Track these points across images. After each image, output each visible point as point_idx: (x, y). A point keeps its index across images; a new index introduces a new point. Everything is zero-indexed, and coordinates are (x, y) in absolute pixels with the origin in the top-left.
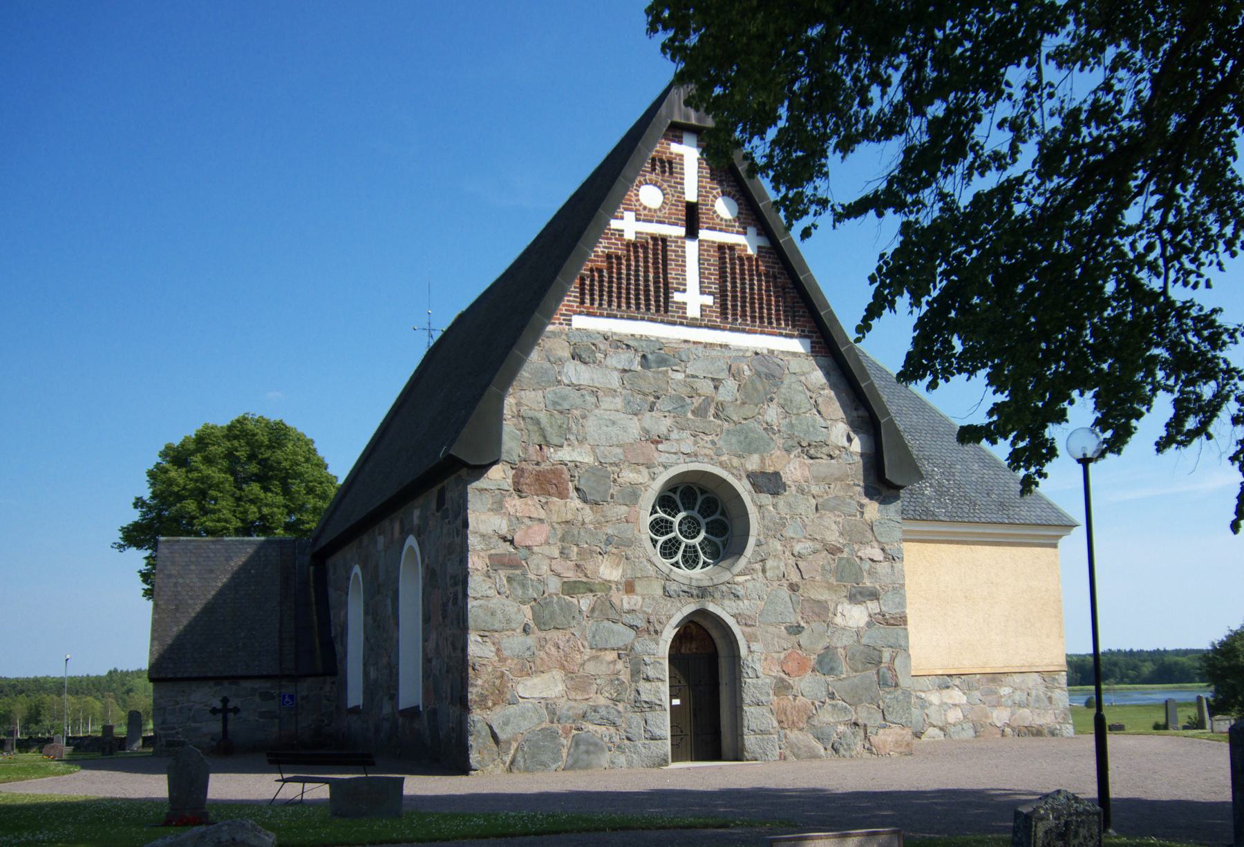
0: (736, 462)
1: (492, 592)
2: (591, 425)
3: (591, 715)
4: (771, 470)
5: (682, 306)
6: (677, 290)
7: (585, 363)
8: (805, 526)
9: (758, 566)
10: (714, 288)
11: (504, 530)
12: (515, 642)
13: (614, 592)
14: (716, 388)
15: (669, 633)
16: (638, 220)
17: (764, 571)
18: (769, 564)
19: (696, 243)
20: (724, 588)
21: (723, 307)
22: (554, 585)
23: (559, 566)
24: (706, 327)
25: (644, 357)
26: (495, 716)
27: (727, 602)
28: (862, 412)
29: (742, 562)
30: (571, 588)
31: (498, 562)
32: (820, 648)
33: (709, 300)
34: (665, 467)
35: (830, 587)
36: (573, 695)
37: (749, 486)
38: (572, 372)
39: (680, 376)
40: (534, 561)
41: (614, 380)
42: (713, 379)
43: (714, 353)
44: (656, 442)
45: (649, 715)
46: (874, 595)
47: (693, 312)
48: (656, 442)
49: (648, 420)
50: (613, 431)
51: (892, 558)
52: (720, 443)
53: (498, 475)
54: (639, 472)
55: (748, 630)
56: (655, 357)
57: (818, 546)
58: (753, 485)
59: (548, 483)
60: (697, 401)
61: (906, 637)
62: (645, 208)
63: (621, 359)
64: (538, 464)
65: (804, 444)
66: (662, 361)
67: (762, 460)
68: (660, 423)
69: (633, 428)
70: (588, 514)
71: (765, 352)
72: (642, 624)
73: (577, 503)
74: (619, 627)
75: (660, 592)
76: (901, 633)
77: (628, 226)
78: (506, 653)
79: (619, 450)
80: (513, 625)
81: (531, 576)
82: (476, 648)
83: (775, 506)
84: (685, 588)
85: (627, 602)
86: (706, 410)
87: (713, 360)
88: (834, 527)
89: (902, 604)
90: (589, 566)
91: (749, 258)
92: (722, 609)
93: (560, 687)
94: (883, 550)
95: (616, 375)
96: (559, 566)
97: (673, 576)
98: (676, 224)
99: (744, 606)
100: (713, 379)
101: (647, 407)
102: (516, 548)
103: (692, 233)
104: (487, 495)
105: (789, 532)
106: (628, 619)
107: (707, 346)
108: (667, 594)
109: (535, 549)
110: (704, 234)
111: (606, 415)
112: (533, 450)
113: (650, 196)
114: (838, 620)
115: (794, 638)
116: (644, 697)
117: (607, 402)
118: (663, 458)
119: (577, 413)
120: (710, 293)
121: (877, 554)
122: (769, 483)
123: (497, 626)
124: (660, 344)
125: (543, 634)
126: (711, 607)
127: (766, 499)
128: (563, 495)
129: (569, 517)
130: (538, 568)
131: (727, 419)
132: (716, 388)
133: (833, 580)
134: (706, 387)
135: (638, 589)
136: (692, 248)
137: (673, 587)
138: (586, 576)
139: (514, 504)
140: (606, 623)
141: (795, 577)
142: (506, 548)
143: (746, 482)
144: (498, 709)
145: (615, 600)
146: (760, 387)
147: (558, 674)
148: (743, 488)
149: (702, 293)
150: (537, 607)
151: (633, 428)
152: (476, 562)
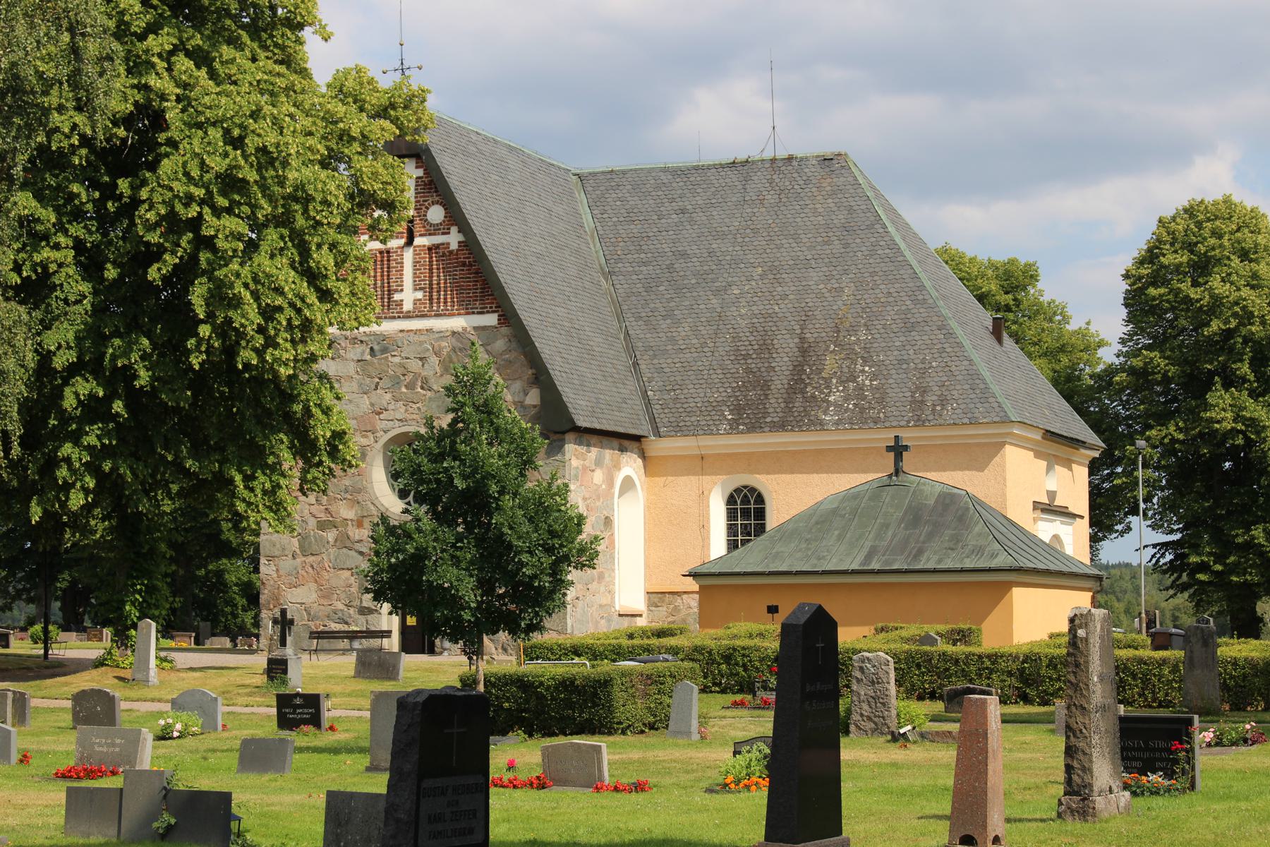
5: (400, 303)
6: (396, 291)
12: (287, 564)
19: (411, 249)
21: (431, 299)
22: (312, 523)
25: (372, 349)
30: (322, 526)
33: (420, 295)
36: (322, 601)
39: (397, 360)
41: (351, 368)
43: (422, 338)
45: (369, 617)
47: (408, 306)
49: (374, 396)
54: (366, 437)
60: (409, 378)
66: (385, 350)
69: (365, 402)
74: (352, 553)
78: (281, 573)
87: (421, 343)
91: (451, 252)
93: (314, 596)
96: (314, 509)
100: (421, 359)
103: (410, 242)
106: (357, 546)
110: (418, 241)
118: (384, 425)
123: (277, 553)
131: (430, 389)
134: (415, 365)
136: (408, 255)
140: (345, 550)
145: (350, 533)
147: (313, 586)
151: (365, 402)
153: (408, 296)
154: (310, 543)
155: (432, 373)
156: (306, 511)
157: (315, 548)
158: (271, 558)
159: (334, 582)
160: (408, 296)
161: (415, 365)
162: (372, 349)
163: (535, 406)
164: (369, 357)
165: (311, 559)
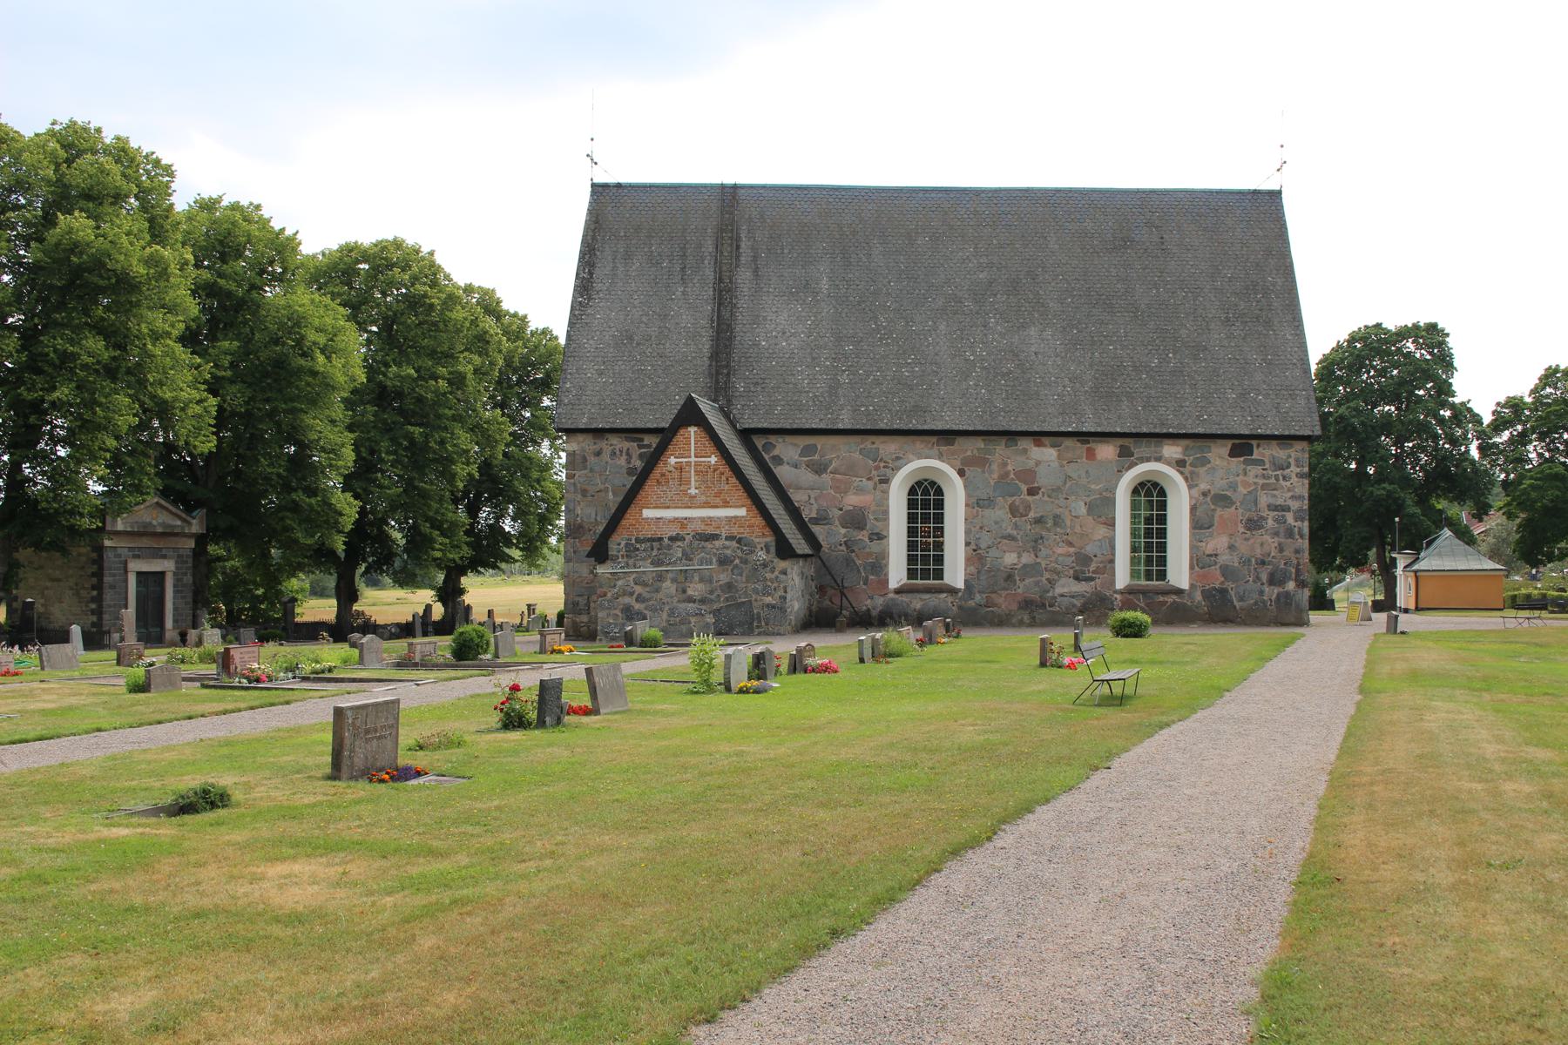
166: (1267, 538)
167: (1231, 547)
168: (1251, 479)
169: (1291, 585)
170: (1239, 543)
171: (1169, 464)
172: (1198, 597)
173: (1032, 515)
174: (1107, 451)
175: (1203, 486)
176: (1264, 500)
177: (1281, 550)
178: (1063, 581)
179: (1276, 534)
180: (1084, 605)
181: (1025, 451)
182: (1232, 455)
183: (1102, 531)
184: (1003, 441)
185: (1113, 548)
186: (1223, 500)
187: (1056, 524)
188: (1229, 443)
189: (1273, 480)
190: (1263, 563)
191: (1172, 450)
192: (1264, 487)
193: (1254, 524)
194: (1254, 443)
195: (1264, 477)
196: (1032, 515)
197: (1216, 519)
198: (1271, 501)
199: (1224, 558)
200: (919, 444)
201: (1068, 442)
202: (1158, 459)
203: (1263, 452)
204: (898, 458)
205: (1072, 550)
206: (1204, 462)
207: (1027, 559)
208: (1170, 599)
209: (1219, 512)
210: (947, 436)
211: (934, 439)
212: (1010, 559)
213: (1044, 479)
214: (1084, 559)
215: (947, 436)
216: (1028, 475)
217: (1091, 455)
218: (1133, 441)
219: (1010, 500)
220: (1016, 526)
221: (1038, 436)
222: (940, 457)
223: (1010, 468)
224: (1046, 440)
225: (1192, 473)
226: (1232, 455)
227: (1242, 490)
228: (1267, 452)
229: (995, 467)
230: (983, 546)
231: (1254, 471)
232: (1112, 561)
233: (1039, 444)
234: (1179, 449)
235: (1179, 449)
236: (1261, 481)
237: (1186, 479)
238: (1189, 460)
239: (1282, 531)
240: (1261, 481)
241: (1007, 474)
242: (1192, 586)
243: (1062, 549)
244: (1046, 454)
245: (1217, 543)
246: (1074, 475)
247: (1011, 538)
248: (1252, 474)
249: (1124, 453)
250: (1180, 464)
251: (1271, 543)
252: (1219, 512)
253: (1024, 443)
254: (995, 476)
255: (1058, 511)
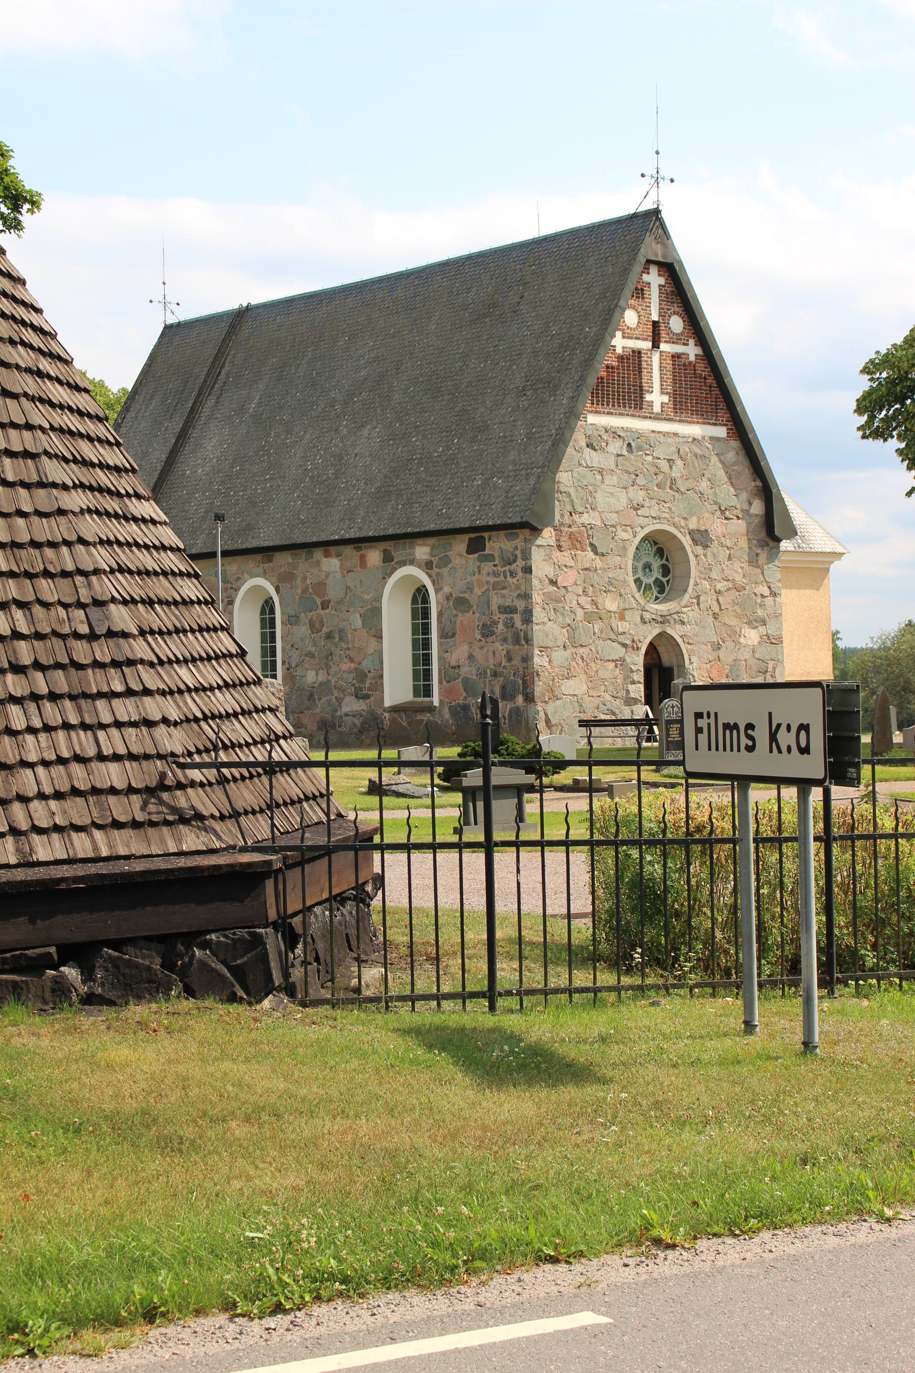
0: (683, 523)
1: (546, 620)
2: (599, 496)
3: (601, 706)
4: (703, 528)
5: (651, 404)
6: (648, 391)
7: (595, 450)
8: (723, 570)
9: (695, 601)
10: (670, 389)
11: (551, 576)
12: (560, 656)
13: (613, 620)
14: (671, 467)
15: (643, 651)
16: (624, 337)
17: (698, 604)
18: (702, 598)
20: (675, 616)
22: (580, 614)
23: (583, 600)
24: (665, 419)
25: (629, 445)
26: (550, 708)
27: (678, 627)
28: (759, 483)
29: (686, 597)
31: (550, 599)
32: (730, 660)
34: (642, 528)
35: (738, 617)
37: (690, 541)
38: (588, 458)
39: (649, 458)
40: (569, 597)
41: (610, 462)
42: (669, 460)
43: (670, 440)
44: (636, 509)
46: (764, 623)
47: (657, 408)
48: (636, 509)
50: (612, 500)
51: (774, 594)
52: (674, 509)
53: (548, 535)
54: (626, 531)
55: (689, 647)
56: (633, 444)
57: (731, 585)
58: (693, 540)
59: (576, 542)
61: (782, 653)
62: (628, 328)
63: (616, 447)
64: (570, 526)
65: (723, 508)
67: (699, 519)
68: (639, 496)
70: (598, 562)
71: (700, 438)
72: (628, 642)
73: (591, 555)
74: (615, 645)
75: (639, 619)
76: (779, 649)
77: (619, 343)
78: (554, 663)
79: (614, 515)
80: (559, 644)
81: (567, 608)
82: (539, 661)
83: (705, 555)
84: (654, 616)
85: (622, 626)
86: (665, 484)
88: (740, 571)
89: (780, 629)
90: (600, 601)
92: (675, 631)
93: (585, 687)
94: (769, 588)
95: (613, 458)
96: (583, 600)
97: (647, 608)
98: (646, 339)
99: (687, 628)
100: (669, 460)
101: (630, 482)
102: (558, 588)
104: (541, 549)
105: (714, 575)
106: (621, 639)
107: (665, 434)
108: (644, 621)
109: (569, 588)
111: (609, 489)
112: (567, 515)
113: (630, 318)
114: (742, 640)
115: (715, 654)
116: (632, 695)
117: (608, 479)
118: (641, 521)
119: (590, 488)
120: (667, 393)
121: (766, 592)
122: (701, 538)
123: (550, 644)
124: (639, 435)
125: (574, 650)
126: (669, 631)
127: (699, 550)
128: (583, 550)
129: (587, 565)
130: (571, 603)
131: (678, 491)
132: (671, 467)
133: (739, 610)
134: (664, 466)
135: (627, 618)
137: (647, 616)
138: (597, 608)
139: (556, 554)
141: (716, 608)
142: (552, 589)
143: (688, 537)
144: (551, 702)
145: (614, 626)
146: (697, 465)
147: (583, 677)
148: (686, 541)
149: (662, 393)
150: (571, 630)
152: (537, 597)
153: (657, 398)
154: (580, 634)
155: (679, 475)
156: (575, 602)
157: (584, 640)
158: (544, 649)
159: (601, 674)
160: (657, 398)
161: (664, 466)
162: (629, 445)
163: (757, 515)
164: (625, 453)
165: (581, 650)
166: (498, 644)
167: (471, 657)
168: (484, 578)
169: (520, 699)
170: (478, 654)
171: (419, 567)
172: (447, 714)
173: (325, 630)
174: (374, 556)
175: (447, 589)
176: (496, 601)
177: (509, 658)
178: (347, 699)
179: (505, 640)
180: (362, 723)
181: (318, 563)
182: (470, 551)
183: (373, 644)
184: (303, 553)
185: (382, 663)
186: (462, 603)
187: (341, 639)
188: (466, 537)
189: (502, 578)
190: (495, 674)
191: (422, 551)
192: (495, 586)
193: (487, 631)
194: (486, 535)
195: (496, 574)
196: (325, 630)
197: (458, 625)
198: (501, 601)
199: (465, 671)
200: (251, 562)
201: (348, 550)
202: (412, 562)
203: (497, 544)
204: (239, 579)
205: (352, 665)
206: (445, 561)
207: (322, 677)
208: (426, 717)
209: (460, 618)
210: (267, 552)
211: (259, 557)
212: (311, 677)
213: (334, 592)
214: (361, 675)
215: (267, 552)
216: (320, 587)
217: (363, 559)
218: (395, 541)
219: (310, 615)
220: (315, 644)
221: (325, 545)
222: (265, 575)
223: (309, 582)
224: (332, 549)
225: (438, 574)
226: (470, 551)
227: (478, 591)
228: (496, 545)
229: (299, 581)
230: (293, 665)
231: (488, 567)
232: (381, 677)
233: (327, 555)
234: (427, 549)
235: (427, 549)
236: (492, 580)
237: (433, 582)
238: (435, 560)
239: (509, 636)
240: (492, 580)
241: (307, 587)
242: (441, 702)
243: (346, 666)
244: (331, 564)
245: (459, 653)
246: (352, 586)
247: (311, 655)
248: (484, 572)
249: (387, 558)
250: (428, 566)
251: (501, 648)
252: (460, 618)
253: (318, 554)
254: (299, 591)
255: (342, 625)
